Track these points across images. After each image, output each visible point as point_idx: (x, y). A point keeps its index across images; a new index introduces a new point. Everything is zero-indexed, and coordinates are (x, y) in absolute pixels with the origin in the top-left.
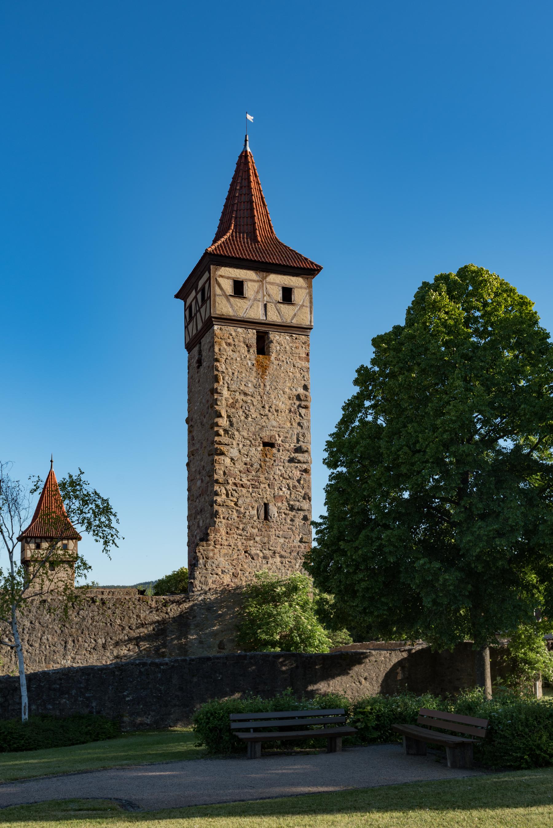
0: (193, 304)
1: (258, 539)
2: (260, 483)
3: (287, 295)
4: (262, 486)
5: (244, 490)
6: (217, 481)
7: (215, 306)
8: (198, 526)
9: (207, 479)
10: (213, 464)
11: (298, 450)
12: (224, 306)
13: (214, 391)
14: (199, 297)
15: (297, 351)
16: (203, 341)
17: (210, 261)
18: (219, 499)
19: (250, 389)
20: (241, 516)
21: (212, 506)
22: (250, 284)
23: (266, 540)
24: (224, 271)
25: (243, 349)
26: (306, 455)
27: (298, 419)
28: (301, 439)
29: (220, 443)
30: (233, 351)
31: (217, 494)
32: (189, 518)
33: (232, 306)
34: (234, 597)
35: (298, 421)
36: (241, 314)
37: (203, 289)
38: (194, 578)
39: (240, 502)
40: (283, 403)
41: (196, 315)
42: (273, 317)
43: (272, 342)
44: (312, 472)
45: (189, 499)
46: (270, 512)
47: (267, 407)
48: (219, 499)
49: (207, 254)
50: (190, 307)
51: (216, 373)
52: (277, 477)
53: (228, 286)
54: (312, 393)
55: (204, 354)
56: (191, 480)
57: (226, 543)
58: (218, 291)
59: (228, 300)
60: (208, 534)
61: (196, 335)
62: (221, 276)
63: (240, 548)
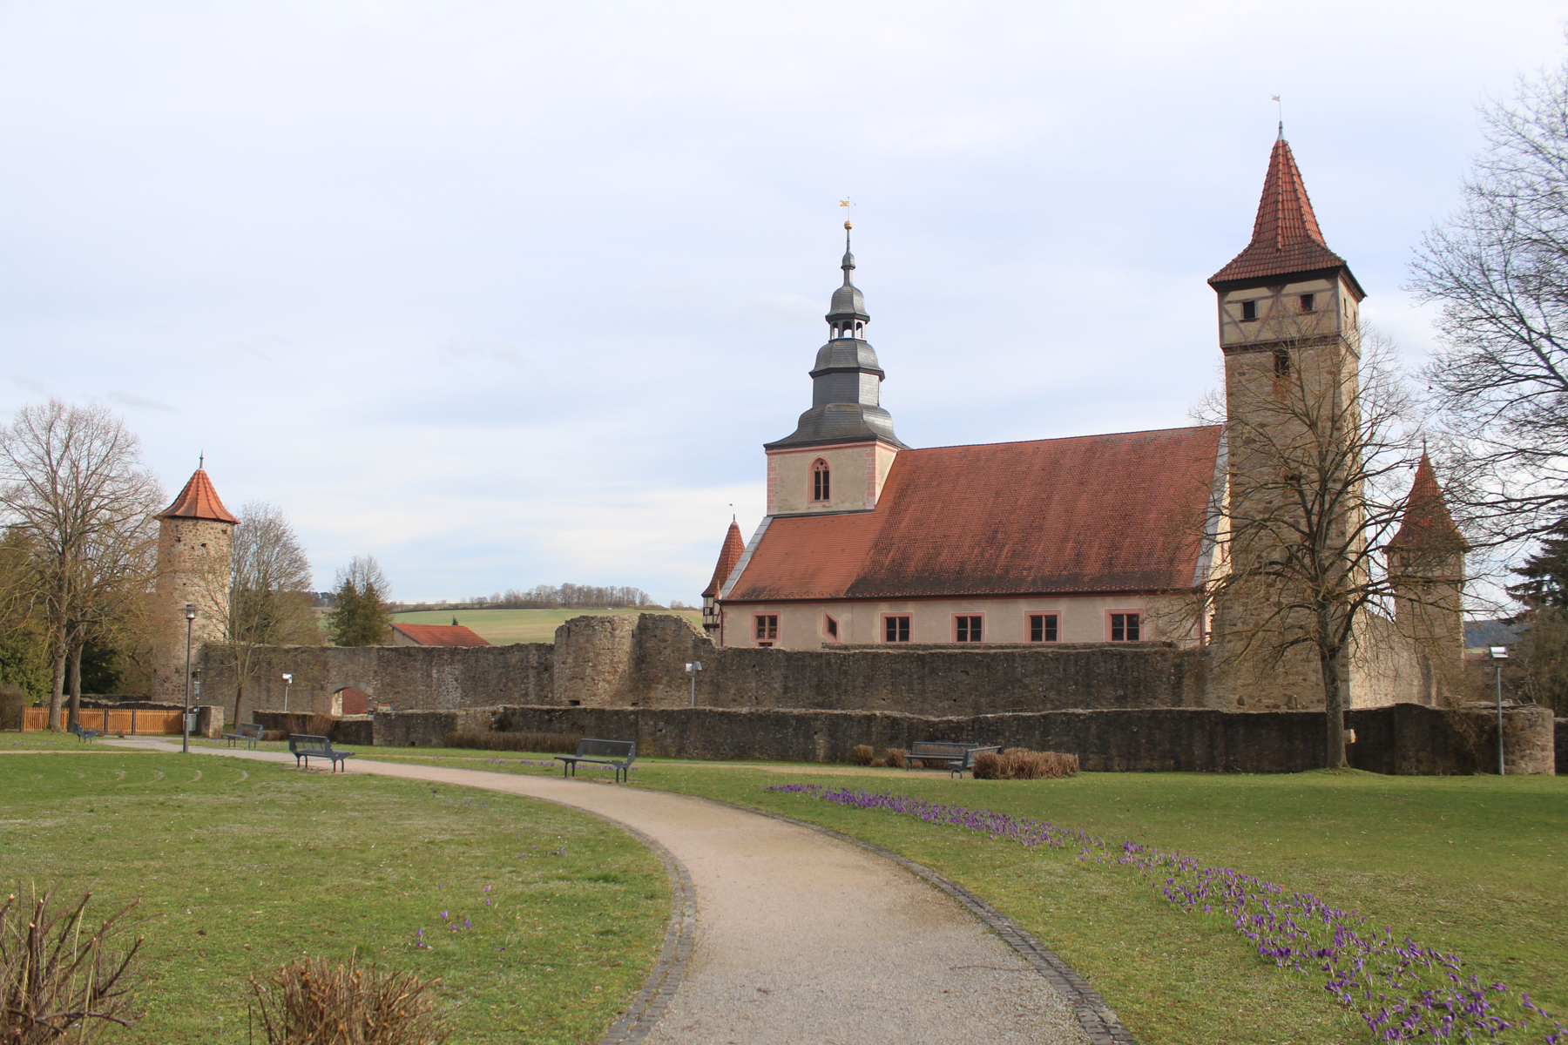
36: (1252, 339)
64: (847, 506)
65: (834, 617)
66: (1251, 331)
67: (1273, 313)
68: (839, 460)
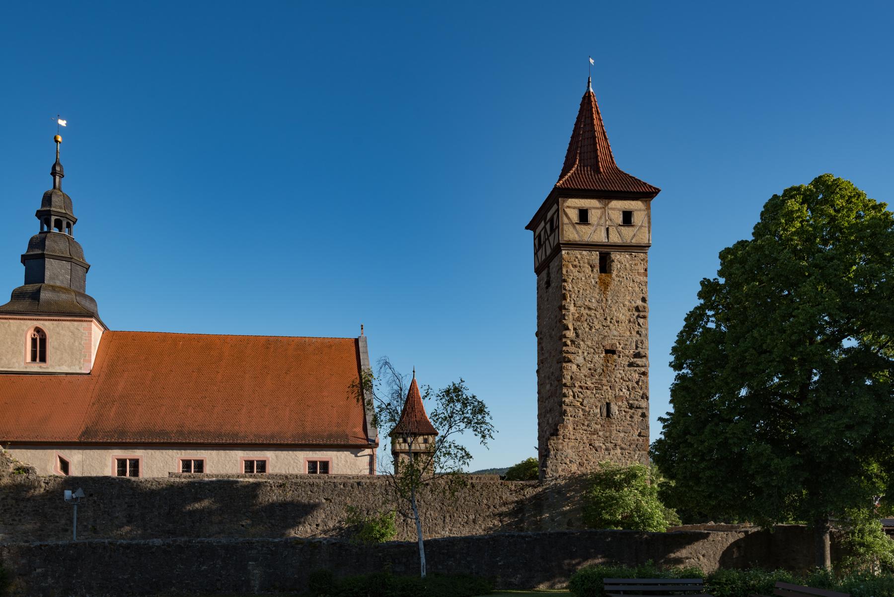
0: (542, 233)
1: (601, 433)
2: (602, 385)
4: (605, 388)
5: (589, 392)
6: (565, 385)
7: (563, 234)
8: (548, 423)
9: (556, 383)
10: (561, 370)
11: (638, 355)
12: (570, 233)
13: (562, 307)
14: (548, 226)
15: (636, 267)
16: (552, 265)
17: (559, 194)
18: (567, 400)
19: (594, 304)
20: (586, 414)
21: (561, 406)
22: (593, 211)
24: (571, 202)
25: (588, 269)
26: (644, 359)
27: (637, 328)
28: (640, 345)
30: (579, 272)
31: (565, 396)
32: (540, 416)
33: (577, 232)
34: (580, 482)
35: (636, 330)
36: (586, 239)
37: (552, 220)
38: (546, 467)
39: (585, 402)
40: (623, 315)
41: (545, 242)
42: (615, 238)
43: (613, 261)
44: (649, 374)
45: (539, 400)
47: (609, 319)
48: (567, 400)
49: (556, 188)
50: (539, 235)
51: (564, 292)
52: (617, 380)
53: (574, 215)
54: (650, 305)
55: (552, 276)
56: (541, 384)
57: (573, 437)
59: (574, 228)
60: (557, 430)
62: (568, 207)
63: (585, 441)
64: (65, 369)
66: (587, 234)
67: (602, 221)
68: (58, 331)
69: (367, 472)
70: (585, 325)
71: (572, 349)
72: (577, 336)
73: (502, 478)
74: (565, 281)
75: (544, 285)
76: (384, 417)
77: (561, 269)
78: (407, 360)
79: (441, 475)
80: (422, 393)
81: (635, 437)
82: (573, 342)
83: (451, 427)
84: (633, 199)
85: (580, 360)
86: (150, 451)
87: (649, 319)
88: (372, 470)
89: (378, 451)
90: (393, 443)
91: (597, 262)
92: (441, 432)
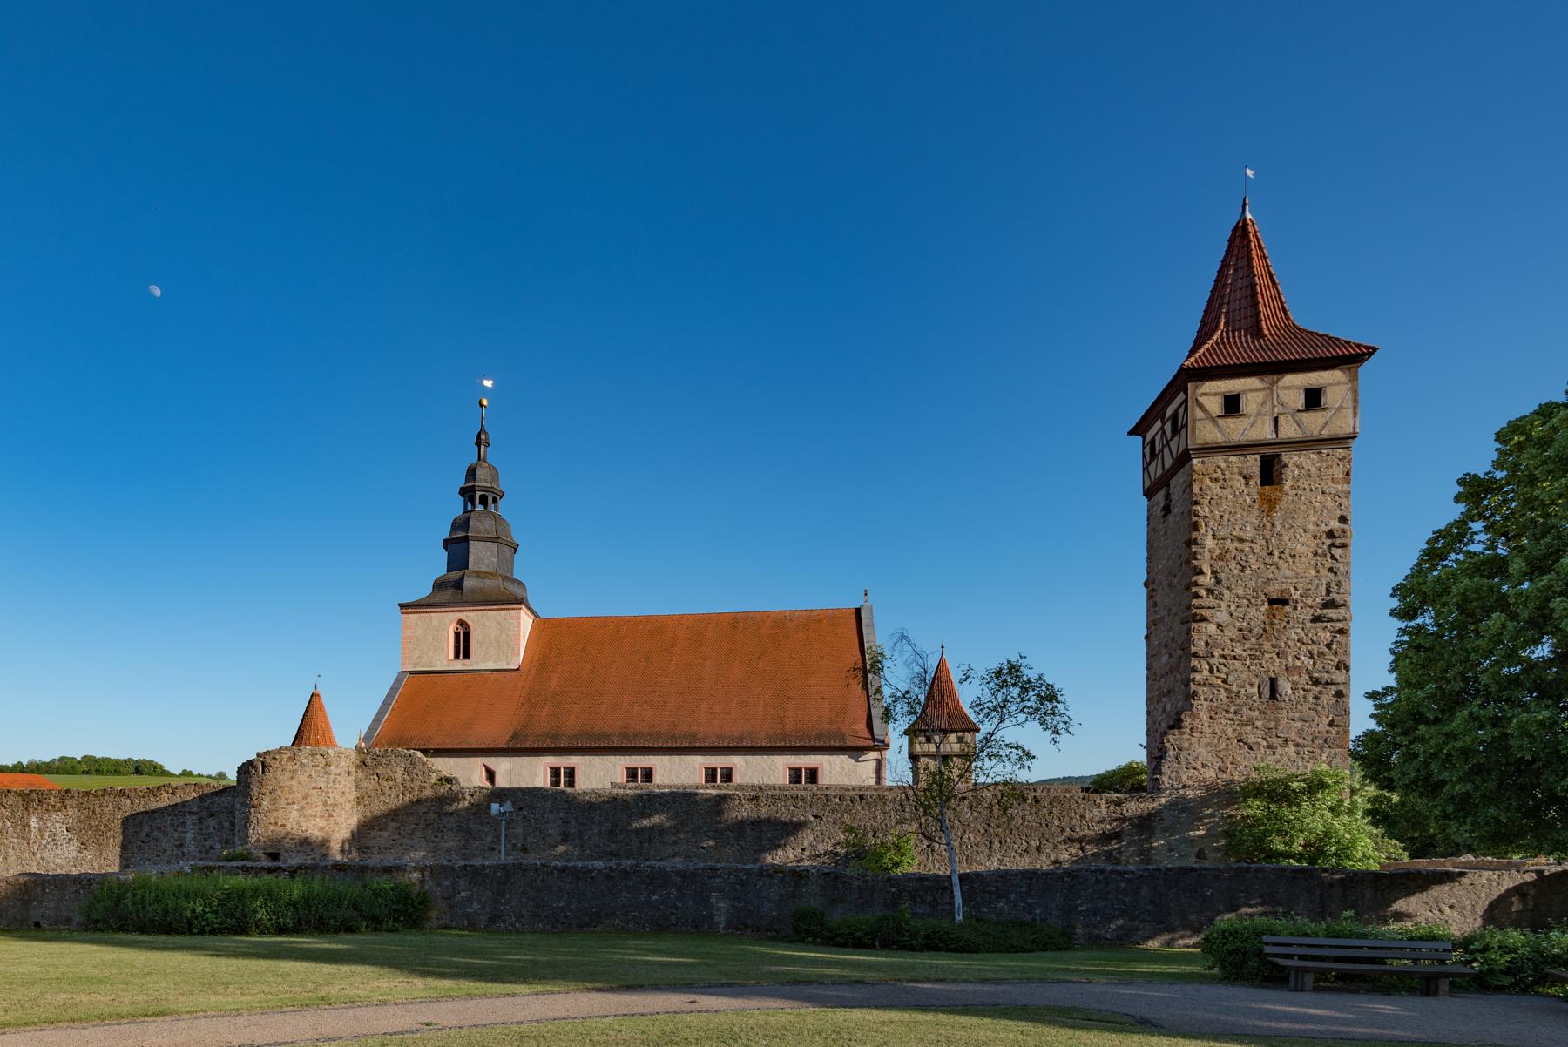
0: (1158, 438)
1: (1258, 724)
3: (1314, 399)
6: (1195, 655)
7: (1194, 435)
8: (1164, 711)
12: (1206, 433)
13: (1190, 543)
14: (1168, 427)
15: (1330, 472)
16: (1173, 482)
17: (1186, 377)
18: (1198, 677)
19: (1249, 532)
21: (1187, 685)
22: (1250, 395)
23: (1272, 724)
25: (1239, 483)
26: (1342, 610)
28: (1334, 589)
29: (1201, 607)
31: (1194, 670)
32: (1149, 701)
33: (1221, 430)
36: (1236, 438)
37: (1175, 417)
39: (1231, 678)
40: (1303, 545)
41: (1161, 451)
42: (1289, 430)
44: (1352, 632)
46: (1280, 689)
47: (1276, 553)
48: (1198, 677)
50: (1153, 442)
53: (1215, 405)
54: (1353, 526)
55: (1174, 498)
56: (1151, 656)
58: (1199, 414)
60: (1181, 721)
61: (1162, 476)
65: (492, 767)
66: (1235, 430)
69: (872, 782)
70: (1233, 565)
71: (1210, 601)
72: (1218, 581)
73: (1086, 790)
74: (1196, 503)
75: (1158, 511)
76: (900, 708)
77: (1191, 485)
78: (934, 628)
79: (987, 786)
80: (955, 675)
81: (1323, 726)
82: (1210, 591)
83: (1002, 720)
84: (1325, 369)
85: (1223, 617)
86: (588, 758)
87: (1352, 548)
88: (879, 779)
89: (889, 755)
90: (911, 744)
91: (1256, 470)
92: (985, 728)
